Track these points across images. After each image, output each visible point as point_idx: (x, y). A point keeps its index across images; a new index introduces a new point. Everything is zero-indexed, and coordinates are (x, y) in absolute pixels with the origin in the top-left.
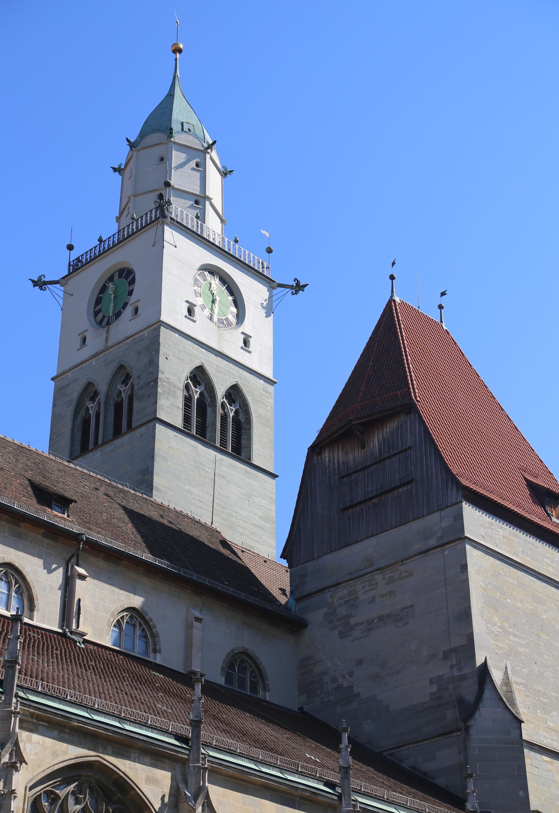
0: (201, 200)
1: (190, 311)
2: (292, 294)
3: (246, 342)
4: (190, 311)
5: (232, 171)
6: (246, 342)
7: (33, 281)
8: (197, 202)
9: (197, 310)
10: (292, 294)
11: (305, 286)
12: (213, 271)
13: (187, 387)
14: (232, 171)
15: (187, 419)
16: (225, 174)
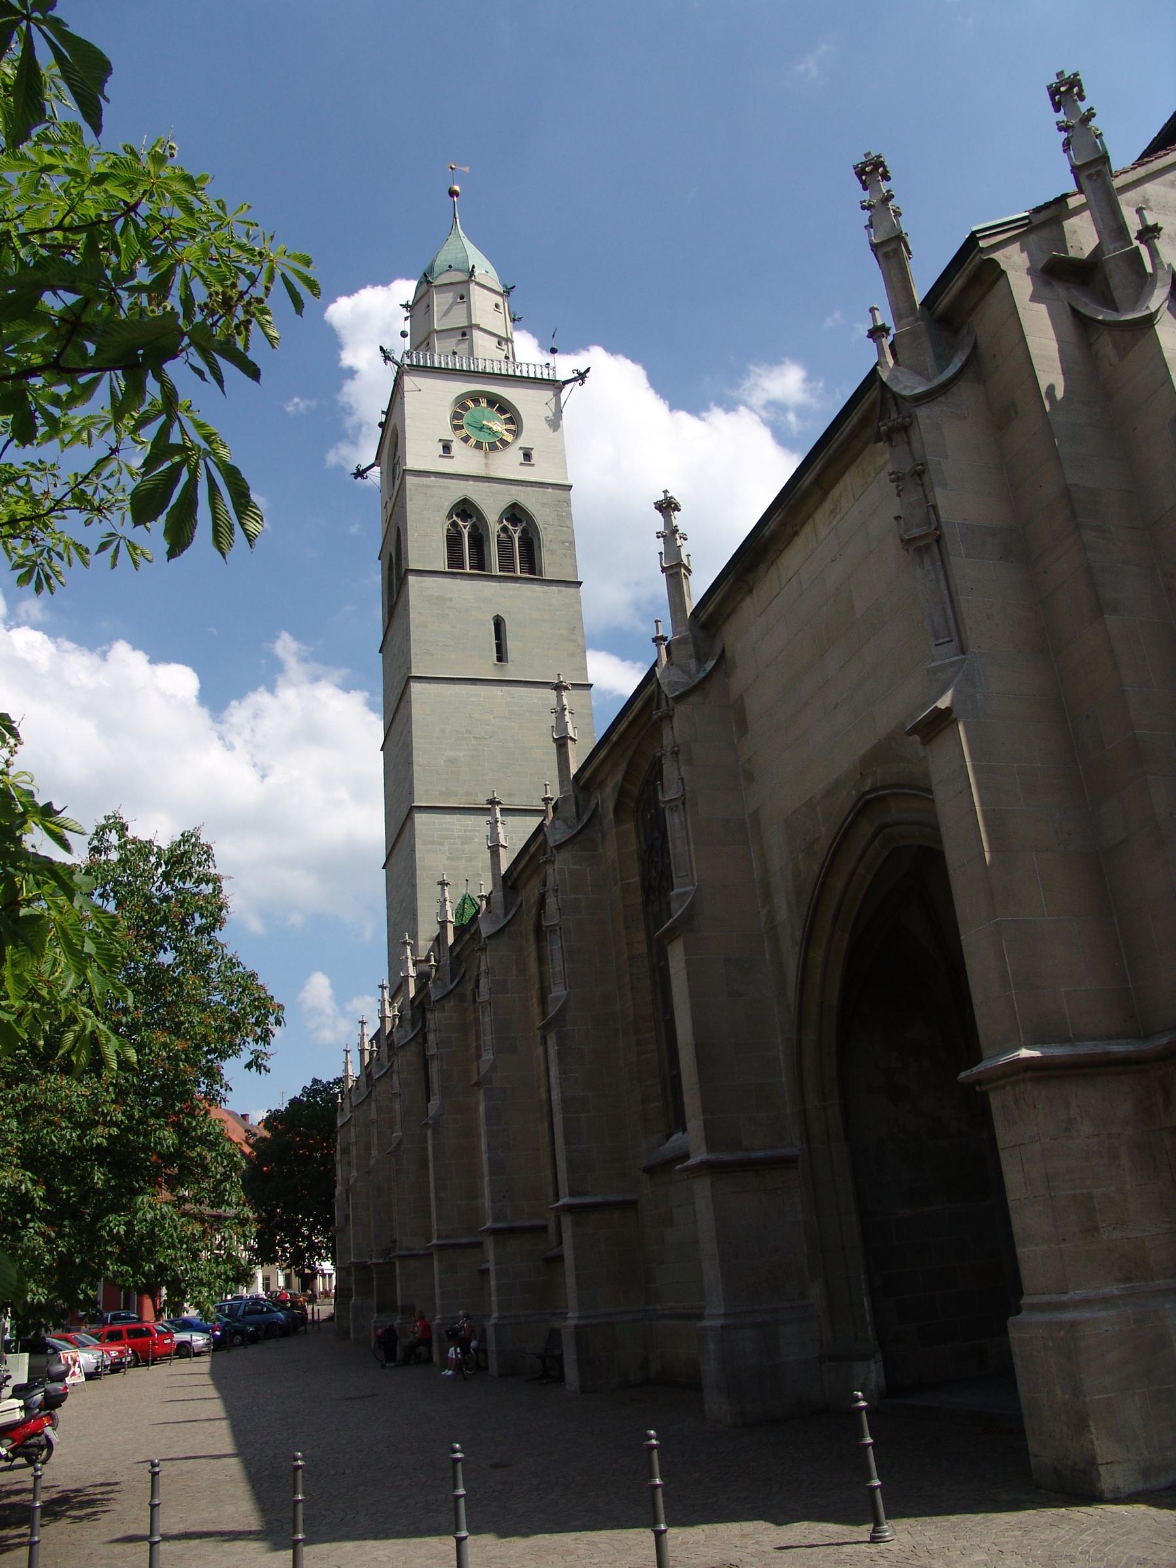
0: (467, 330)
1: (447, 448)
2: (580, 385)
3: (527, 456)
4: (447, 448)
5: (514, 287)
6: (527, 456)
7: (354, 474)
8: (464, 334)
9: (457, 446)
10: (580, 385)
11: (588, 370)
12: (476, 397)
13: (454, 524)
14: (514, 287)
15: (455, 559)
16: (507, 292)
